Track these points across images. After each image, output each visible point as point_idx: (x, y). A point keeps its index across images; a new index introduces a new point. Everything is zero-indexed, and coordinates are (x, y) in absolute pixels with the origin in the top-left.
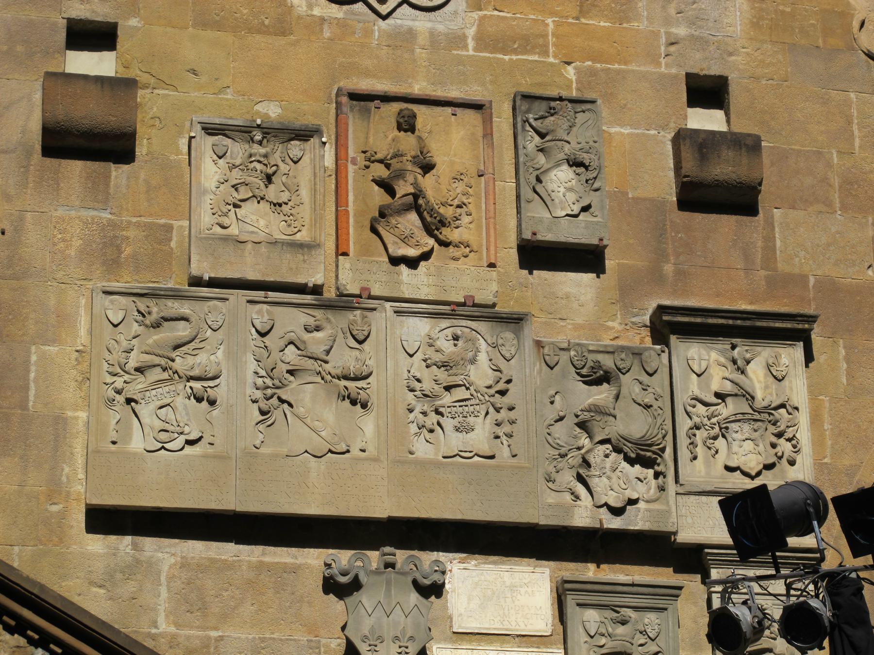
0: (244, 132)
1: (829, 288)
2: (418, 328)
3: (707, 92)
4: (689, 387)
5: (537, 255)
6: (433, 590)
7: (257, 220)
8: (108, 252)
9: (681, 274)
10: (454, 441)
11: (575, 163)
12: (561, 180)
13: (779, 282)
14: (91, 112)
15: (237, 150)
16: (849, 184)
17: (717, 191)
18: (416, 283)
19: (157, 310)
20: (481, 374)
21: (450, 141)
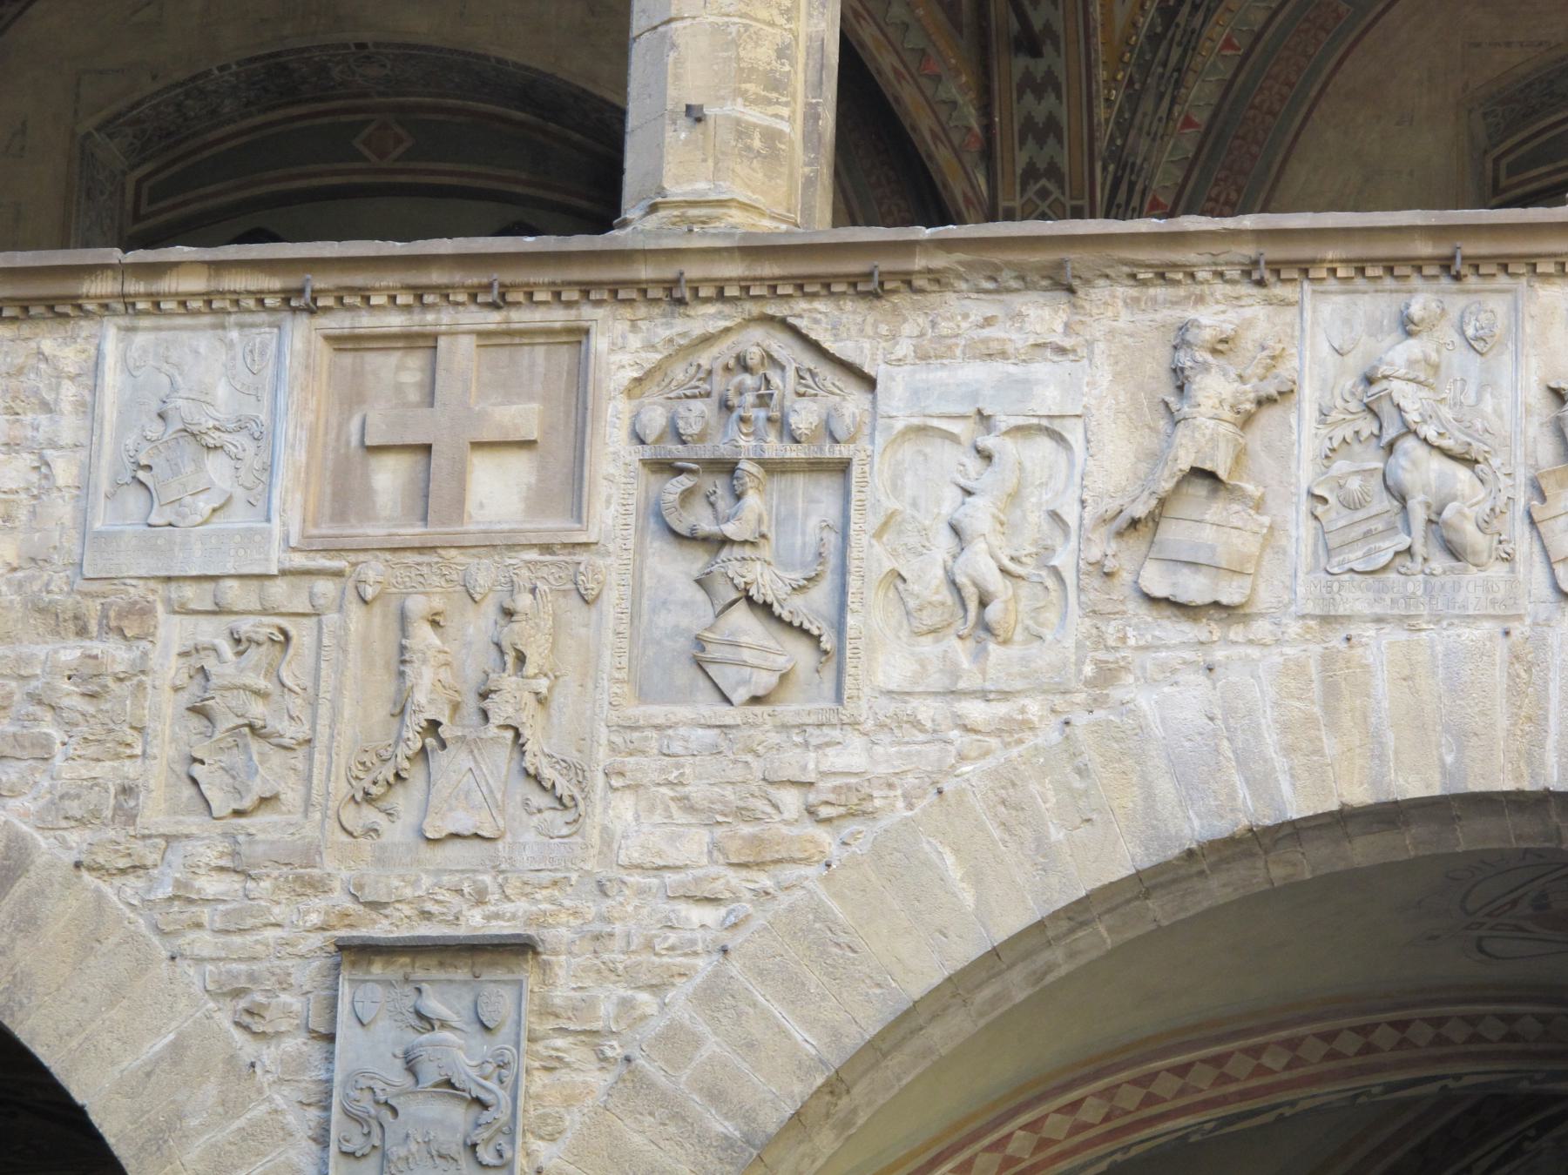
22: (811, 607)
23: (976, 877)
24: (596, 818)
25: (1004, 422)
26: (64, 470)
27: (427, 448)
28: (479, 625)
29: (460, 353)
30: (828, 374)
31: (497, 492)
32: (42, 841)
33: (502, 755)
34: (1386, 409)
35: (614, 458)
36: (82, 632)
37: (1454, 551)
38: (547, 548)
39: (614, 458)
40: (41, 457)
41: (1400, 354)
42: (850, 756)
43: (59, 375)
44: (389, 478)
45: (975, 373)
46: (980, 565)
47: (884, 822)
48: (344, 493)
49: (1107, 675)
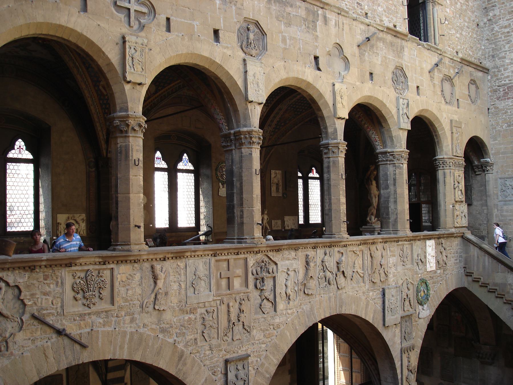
22: (271, 297)
23: (290, 335)
24: (252, 334)
25: (291, 270)
26: (183, 286)
27: (229, 278)
28: (237, 305)
29: (232, 262)
30: (272, 263)
31: (237, 283)
32: (185, 350)
33: (241, 326)
34: (325, 266)
35: (251, 278)
36: (187, 313)
37: (329, 284)
38: (244, 293)
39: (251, 278)
40: (179, 284)
41: (326, 257)
42: (277, 320)
43: (181, 268)
44: (224, 282)
45: (287, 262)
46: (289, 291)
47: (281, 329)
48: (218, 286)
49: (301, 305)
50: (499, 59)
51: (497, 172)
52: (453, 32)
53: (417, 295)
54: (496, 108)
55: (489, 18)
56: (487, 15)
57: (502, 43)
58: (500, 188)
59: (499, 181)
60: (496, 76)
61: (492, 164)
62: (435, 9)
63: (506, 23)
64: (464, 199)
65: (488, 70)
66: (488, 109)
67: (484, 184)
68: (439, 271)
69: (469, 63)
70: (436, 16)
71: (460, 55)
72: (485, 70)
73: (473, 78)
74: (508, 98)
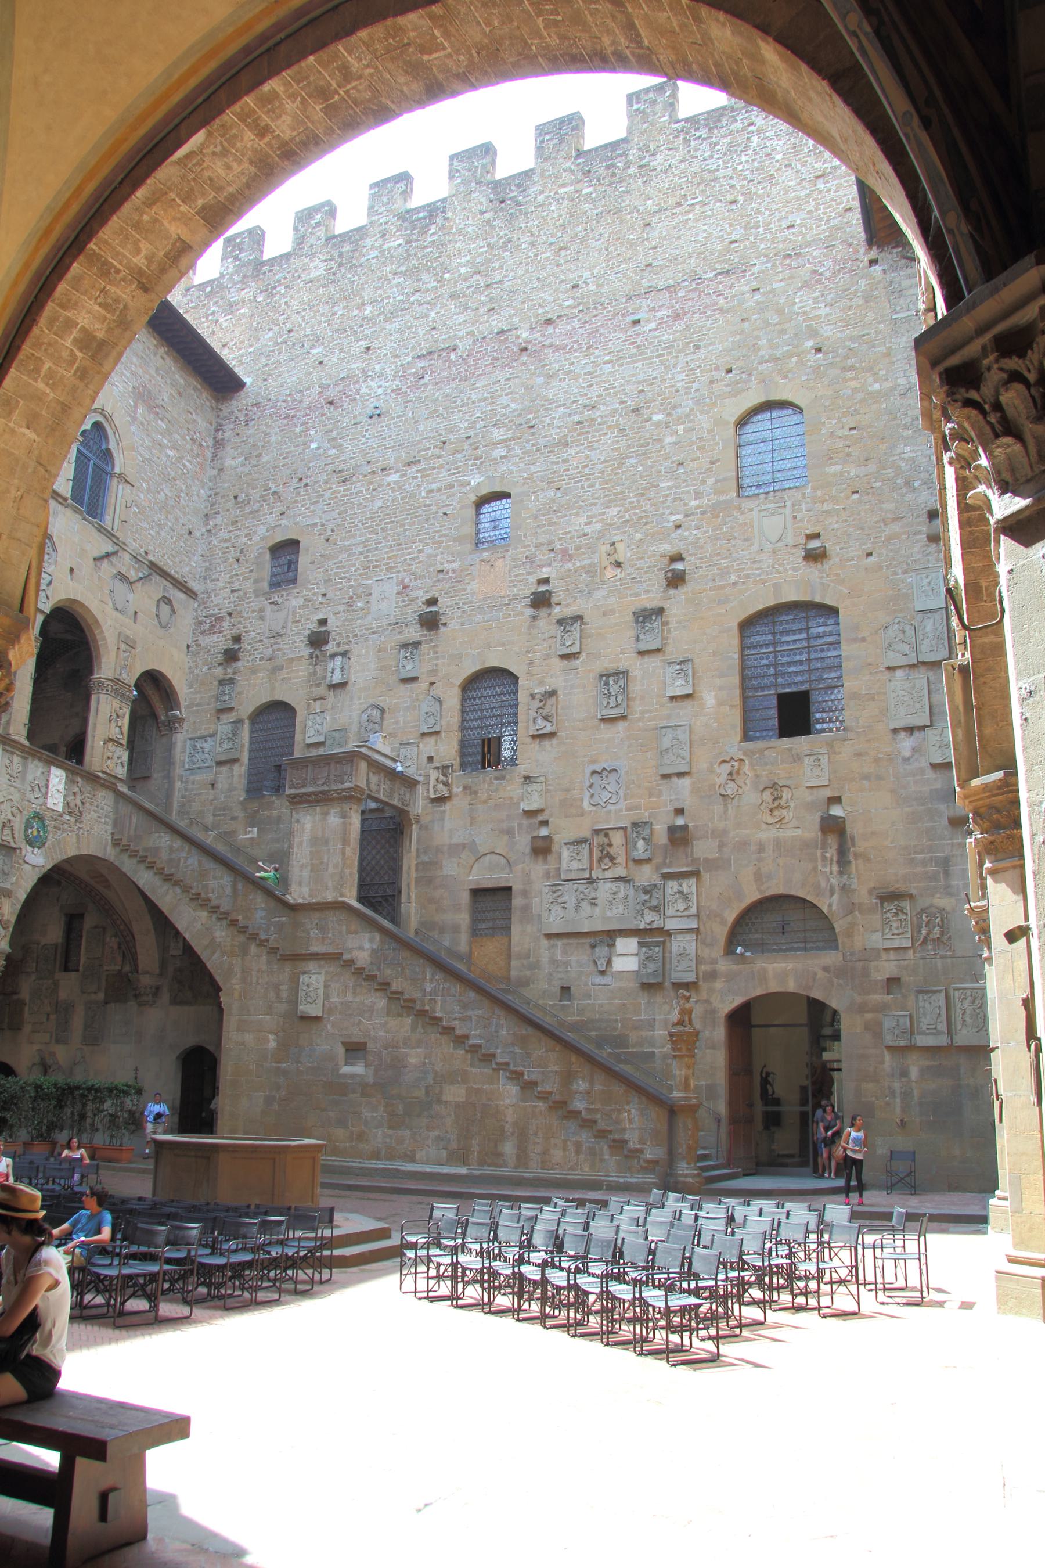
0: (572, 844)
1: (706, 860)
2: (609, 885)
3: (680, 812)
4: (668, 891)
5: (638, 862)
6: (612, 945)
7: (575, 865)
8: (547, 875)
9: (671, 862)
10: (615, 911)
11: (644, 839)
12: (641, 844)
13: (695, 861)
14: (540, 843)
15: (572, 847)
16: (713, 832)
17: (679, 837)
18: (609, 874)
19: (554, 888)
20: (621, 895)
21: (617, 839)
50: (212, 581)
51: (187, 731)
52: (145, 525)
53: (26, 830)
54: (198, 645)
55: (209, 527)
56: (208, 524)
57: (218, 561)
58: (188, 752)
59: (188, 742)
60: (204, 603)
61: (182, 720)
62: (121, 487)
63: (227, 536)
64: (124, 742)
65: (196, 595)
66: (188, 646)
67: (170, 748)
68: (67, 817)
69: (164, 574)
70: (120, 495)
71: (151, 557)
72: (191, 593)
73: (167, 595)
74: (215, 633)
